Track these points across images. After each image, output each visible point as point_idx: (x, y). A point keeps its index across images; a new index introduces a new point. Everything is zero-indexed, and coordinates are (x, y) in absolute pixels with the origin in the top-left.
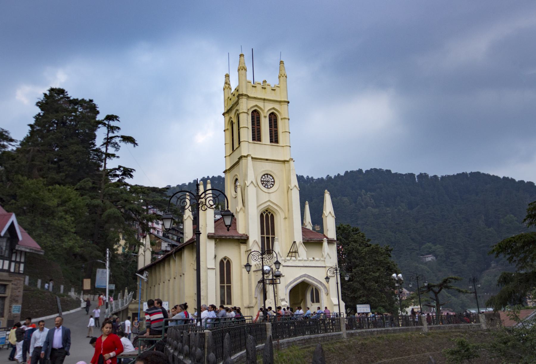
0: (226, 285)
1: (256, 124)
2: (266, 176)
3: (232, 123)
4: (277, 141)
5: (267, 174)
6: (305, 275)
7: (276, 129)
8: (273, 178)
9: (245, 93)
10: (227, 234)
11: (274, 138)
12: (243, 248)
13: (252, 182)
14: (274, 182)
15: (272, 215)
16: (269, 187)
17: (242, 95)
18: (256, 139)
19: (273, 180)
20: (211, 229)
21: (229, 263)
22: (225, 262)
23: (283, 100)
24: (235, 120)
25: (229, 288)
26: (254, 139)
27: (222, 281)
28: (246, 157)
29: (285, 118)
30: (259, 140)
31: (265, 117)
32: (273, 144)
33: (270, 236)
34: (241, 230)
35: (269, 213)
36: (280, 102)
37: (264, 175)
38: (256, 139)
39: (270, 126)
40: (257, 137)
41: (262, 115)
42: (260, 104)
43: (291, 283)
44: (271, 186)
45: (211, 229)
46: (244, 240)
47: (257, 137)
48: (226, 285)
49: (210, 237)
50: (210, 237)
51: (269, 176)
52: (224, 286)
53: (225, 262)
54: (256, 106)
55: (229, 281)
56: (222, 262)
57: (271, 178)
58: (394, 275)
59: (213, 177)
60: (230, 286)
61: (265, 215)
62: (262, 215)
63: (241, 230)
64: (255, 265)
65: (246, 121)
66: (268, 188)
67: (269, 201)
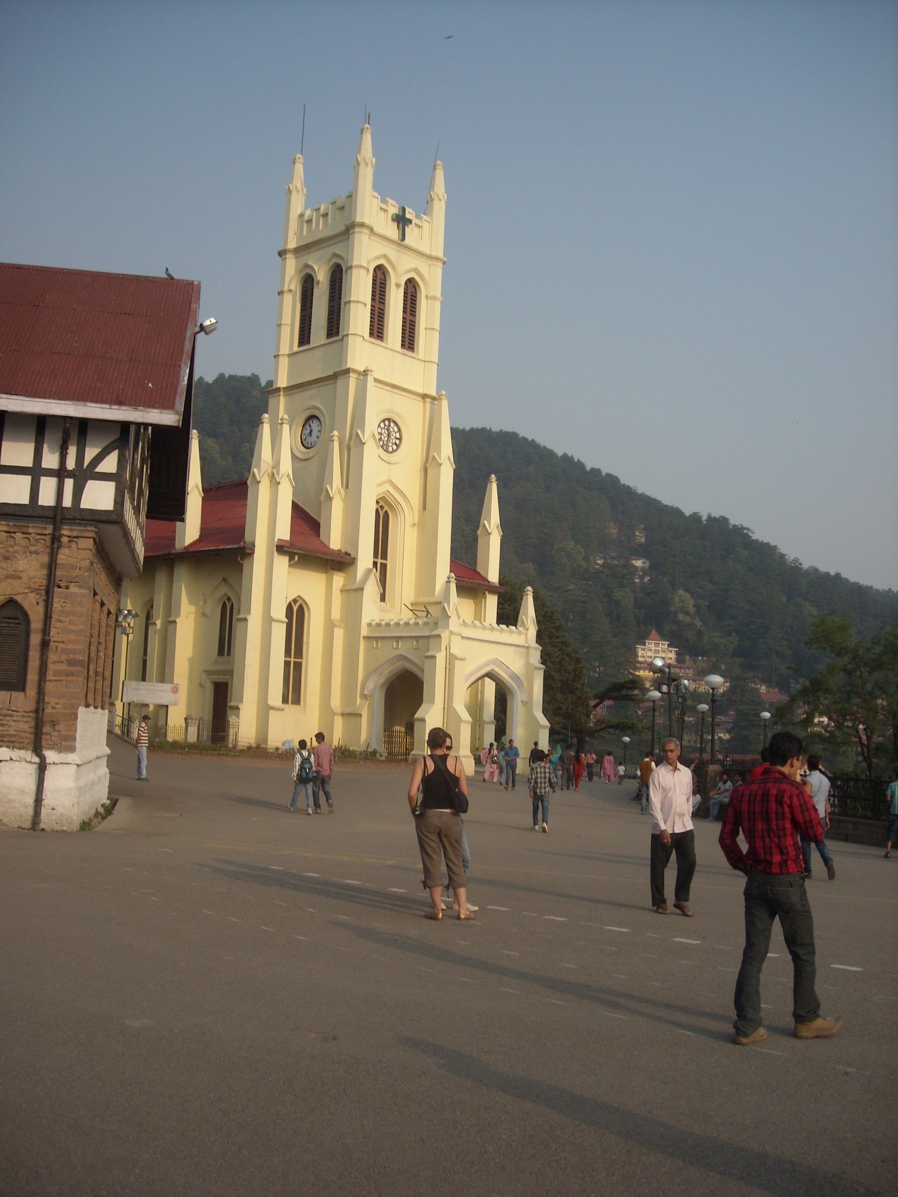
0: (292, 660)
2: (387, 423)
3: (308, 283)
5: (389, 420)
6: (496, 661)
8: (399, 430)
9: (366, 221)
10: (306, 545)
11: (409, 341)
12: (339, 580)
13: (374, 435)
14: (400, 439)
15: (386, 513)
16: (390, 449)
17: (362, 225)
18: (375, 333)
19: (398, 436)
21: (301, 609)
22: (295, 608)
23: (434, 254)
24: (322, 276)
25: (298, 666)
27: (288, 652)
28: (365, 373)
29: (435, 298)
31: (398, 285)
32: (405, 351)
33: (379, 561)
35: (382, 507)
36: (430, 257)
37: (384, 421)
38: (375, 333)
40: (377, 330)
42: (392, 252)
43: (471, 675)
44: (395, 447)
45: (284, 532)
46: (341, 562)
47: (377, 330)
48: (292, 660)
49: (281, 548)
50: (281, 548)
51: (392, 425)
52: (290, 662)
53: (295, 608)
54: (385, 257)
55: (299, 653)
56: (289, 608)
57: (396, 429)
60: (301, 663)
64: (369, 625)
66: (386, 451)
67: (391, 482)
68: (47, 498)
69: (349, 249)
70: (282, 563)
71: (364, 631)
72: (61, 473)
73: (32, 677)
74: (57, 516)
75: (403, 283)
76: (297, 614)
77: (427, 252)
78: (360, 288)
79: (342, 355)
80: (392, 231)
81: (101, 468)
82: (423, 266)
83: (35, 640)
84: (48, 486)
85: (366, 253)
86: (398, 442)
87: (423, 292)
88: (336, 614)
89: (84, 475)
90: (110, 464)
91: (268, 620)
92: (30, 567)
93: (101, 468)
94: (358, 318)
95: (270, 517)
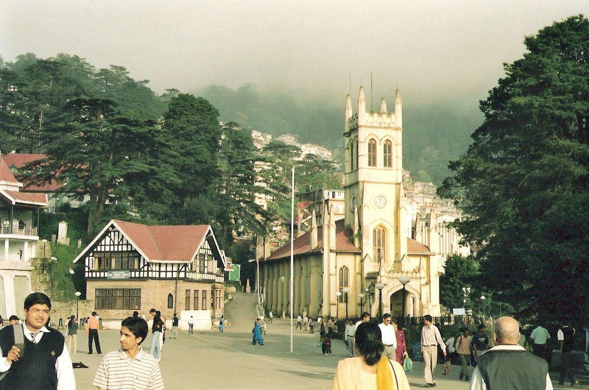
1: (372, 151)
2: (379, 197)
4: (390, 165)
7: (390, 154)
11: (388, 162)
12: (358, 258)
14: (386, 202)
17: (361, 126)
26: (370, 165)
30: (374, 165)
39: (385, 152)
40: (372, 162)
45: (333, 246)
47: (372, 162)
51: (382, 197)
61: (377, 230)
62: (375, 231)
71: (365, 275)
73: (174, 306)
76: (344, 271)
78: (363, 150)
79: (357, 176)
81: (182, 270)
83: (174, 300)
85: (364, 135)
86: (385, 203)
87: (393, 144)
88: (358, 270)
93: (182, 270)
94: (363, 161)
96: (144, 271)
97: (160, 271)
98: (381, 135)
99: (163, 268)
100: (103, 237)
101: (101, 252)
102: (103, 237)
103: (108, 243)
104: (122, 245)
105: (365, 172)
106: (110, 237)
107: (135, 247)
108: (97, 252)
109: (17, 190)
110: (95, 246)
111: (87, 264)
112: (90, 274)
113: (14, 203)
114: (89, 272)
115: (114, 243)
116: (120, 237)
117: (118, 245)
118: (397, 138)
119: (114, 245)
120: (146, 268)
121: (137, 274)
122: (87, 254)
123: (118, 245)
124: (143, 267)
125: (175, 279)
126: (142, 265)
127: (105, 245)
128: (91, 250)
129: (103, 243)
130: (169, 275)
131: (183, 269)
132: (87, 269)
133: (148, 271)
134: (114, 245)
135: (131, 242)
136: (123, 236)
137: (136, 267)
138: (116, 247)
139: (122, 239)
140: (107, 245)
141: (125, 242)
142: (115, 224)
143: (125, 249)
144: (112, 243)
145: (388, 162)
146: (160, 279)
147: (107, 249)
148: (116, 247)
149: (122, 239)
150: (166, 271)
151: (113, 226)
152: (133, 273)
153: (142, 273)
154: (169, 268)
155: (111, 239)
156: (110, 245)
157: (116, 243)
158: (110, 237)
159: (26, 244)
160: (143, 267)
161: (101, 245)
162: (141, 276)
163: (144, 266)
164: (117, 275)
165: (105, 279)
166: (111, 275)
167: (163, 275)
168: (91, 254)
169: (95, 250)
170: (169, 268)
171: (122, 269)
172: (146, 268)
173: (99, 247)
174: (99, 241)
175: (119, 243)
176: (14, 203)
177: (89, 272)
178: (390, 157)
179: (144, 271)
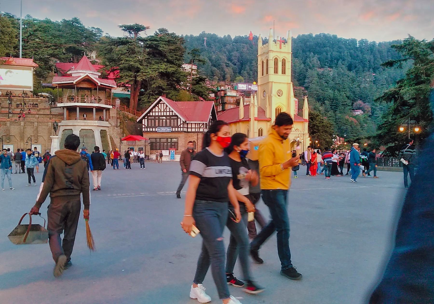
4: (285, 73)
11: (284, 72)
17: (271, 50)
20: (256, 116)
24: (265, 62)
26: (275, 73)
28: (272, 82)
30: (277, 73)
34: (268, 116)
40: (276, 71)
41: (279, 60)
42: (278, 54)
45: (256, 116)
47: (276, 71)
49: (256, 119)
50: (256, 119)
58: (333, 140)
59: (187, 35)
62: (276, 109)
63: (268, 116)
65: (271, 64)
68: (197, 131)
69: (269, 55)
70: (256, 122)
72: (198, 128)
74: (198, 132)
75: (281, 60)
77: (287, 52)
78: (271, 64)
80: (278, 50)
82: (286, 55)
84: (197, 129)
85: (272, 56)
87: (287, 61)
89: (200, 128)
90: (202, 127)
91: (254, 133)
92: (196, 137)
94: (271, 70)
95: (254, 112)
96: (180, 128)
97: (187, 128)
98: (281, 57)
99: (189, 126)
100: (154, 107)
101: (152, 116)
102: (154, 107)
103: (157, 110)
104: (166, 112)
105: (272, 77)
106: (158, 107)
107: (177, 114)
108: (150, 116)
109: (97, 77)
110: (149, 112)
111: (143, 123)
112: (146, 129)
113: (99, 84)
114: (145, 128)
115: (161, 110)
116: (165, 107)
117: (164, 112)
118: (289, 58)
119: (161, 112)
120: (182, 126)
121: (176, 129)
122: (144, 118)
123: (164, 112)
124: (180, 125)
125: (197, 132)
126: (179, 124)
127: (155, 112)
128: (146, 115)
129: (154, 110)
130: (193, 130)
131: (202, 127)
132: (144, 126)
133: (183, 127)
134: (161, 112)
135: (173, 110)
136: (167, 106)
137: (176, 125)
138: (162, 113)
139: (166, 108)
140: (156, 112)
141: (168, 110)
142: (162, 99)
143: (168, 114)
144: (159, 111)
145: (284, 72)
146: (188, 132)
147: (157, 114)
148: (162, 113)
149: (166, 108)
150: (191, 128)
151: (161, 100)
152: (174, 129)
153: (179, 129)
154: (193, 126)
155: (159, 108)
156: (158, 112)
157: (162, 110)
158: (158, 107)
159: (104, 111)
160: (180, 125)
161: (153, 112)
162: (179, 130)
163: (181, 124)
164: (163, 129)
165: (156, 132)
166: (159, 130)
167: (189, 130)
168: (146, 117)
169: (149, 115)
170: (193, 126)
171: (166, 126)
172: (182, 126)
173: (151, 113)
174: (152, 109)
175: (164, 110)
176: (99, 84)
177: (145, 128)
178: (285, 68)
179: (180, 128)
